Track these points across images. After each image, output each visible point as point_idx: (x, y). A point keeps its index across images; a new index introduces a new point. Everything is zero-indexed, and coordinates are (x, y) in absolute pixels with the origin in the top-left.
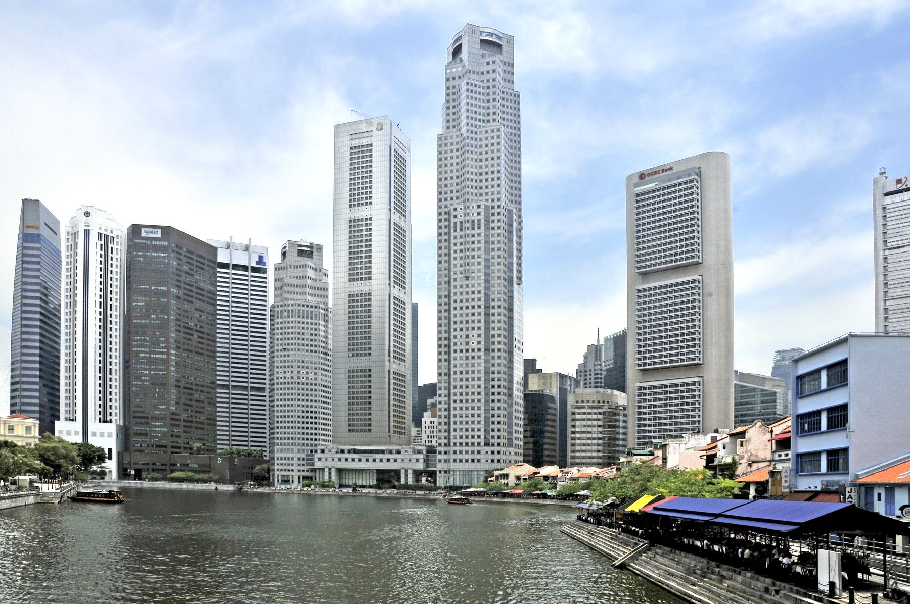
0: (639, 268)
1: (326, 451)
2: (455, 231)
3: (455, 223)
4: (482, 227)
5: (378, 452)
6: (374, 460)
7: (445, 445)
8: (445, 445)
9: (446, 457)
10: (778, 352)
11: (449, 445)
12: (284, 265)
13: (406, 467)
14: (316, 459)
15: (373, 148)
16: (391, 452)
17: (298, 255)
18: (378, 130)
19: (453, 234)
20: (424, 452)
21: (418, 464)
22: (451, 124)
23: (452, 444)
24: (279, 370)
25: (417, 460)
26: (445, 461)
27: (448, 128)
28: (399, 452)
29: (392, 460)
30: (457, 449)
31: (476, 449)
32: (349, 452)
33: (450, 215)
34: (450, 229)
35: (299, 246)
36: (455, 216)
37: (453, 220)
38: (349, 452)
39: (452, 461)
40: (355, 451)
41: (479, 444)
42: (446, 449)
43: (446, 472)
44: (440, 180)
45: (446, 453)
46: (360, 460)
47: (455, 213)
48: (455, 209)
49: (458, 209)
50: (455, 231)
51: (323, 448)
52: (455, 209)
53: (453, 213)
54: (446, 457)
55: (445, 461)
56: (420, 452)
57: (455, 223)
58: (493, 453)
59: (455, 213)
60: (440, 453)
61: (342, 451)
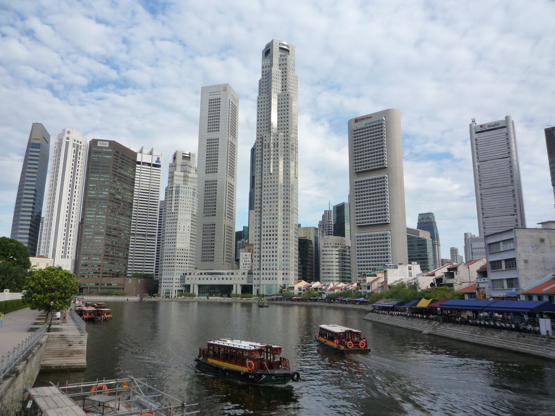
1: (192, 274)
2: (265, 148)
3: (265, 144)
4: (279, 147)
5: (220, 274)
6: (219, 279)
8: (258, 269)
9: (258, 276)
10: (420, 215)
14: (186, 279)
15: (221, 101)
16: (228, 274)
19: (264, 150)
20: (246, 274)
24: (169, 225)
25: (243, 279)
26: (258, 279)
28: (232, 274)
32: (205, 274)
34: (262, 147)
36: (265, 140)
37: (264, 142)
38: (205, 274)
40: (209, 274)
42: (258, 272)
43: (258, 285)
45: (258, 274)
46: (211, 279)
47: (265, 139)
48: (266, 137)
50: (265, 148)
51: (190, 272)
52: (266, 137)
53: (264, 139)
54: (258, 276)
55: (258, 279)
56: (244, 274)
57: (265, 144)
58: (283, 274)
59: (265, 139)
60: (255, 274)
61: (201, 274)
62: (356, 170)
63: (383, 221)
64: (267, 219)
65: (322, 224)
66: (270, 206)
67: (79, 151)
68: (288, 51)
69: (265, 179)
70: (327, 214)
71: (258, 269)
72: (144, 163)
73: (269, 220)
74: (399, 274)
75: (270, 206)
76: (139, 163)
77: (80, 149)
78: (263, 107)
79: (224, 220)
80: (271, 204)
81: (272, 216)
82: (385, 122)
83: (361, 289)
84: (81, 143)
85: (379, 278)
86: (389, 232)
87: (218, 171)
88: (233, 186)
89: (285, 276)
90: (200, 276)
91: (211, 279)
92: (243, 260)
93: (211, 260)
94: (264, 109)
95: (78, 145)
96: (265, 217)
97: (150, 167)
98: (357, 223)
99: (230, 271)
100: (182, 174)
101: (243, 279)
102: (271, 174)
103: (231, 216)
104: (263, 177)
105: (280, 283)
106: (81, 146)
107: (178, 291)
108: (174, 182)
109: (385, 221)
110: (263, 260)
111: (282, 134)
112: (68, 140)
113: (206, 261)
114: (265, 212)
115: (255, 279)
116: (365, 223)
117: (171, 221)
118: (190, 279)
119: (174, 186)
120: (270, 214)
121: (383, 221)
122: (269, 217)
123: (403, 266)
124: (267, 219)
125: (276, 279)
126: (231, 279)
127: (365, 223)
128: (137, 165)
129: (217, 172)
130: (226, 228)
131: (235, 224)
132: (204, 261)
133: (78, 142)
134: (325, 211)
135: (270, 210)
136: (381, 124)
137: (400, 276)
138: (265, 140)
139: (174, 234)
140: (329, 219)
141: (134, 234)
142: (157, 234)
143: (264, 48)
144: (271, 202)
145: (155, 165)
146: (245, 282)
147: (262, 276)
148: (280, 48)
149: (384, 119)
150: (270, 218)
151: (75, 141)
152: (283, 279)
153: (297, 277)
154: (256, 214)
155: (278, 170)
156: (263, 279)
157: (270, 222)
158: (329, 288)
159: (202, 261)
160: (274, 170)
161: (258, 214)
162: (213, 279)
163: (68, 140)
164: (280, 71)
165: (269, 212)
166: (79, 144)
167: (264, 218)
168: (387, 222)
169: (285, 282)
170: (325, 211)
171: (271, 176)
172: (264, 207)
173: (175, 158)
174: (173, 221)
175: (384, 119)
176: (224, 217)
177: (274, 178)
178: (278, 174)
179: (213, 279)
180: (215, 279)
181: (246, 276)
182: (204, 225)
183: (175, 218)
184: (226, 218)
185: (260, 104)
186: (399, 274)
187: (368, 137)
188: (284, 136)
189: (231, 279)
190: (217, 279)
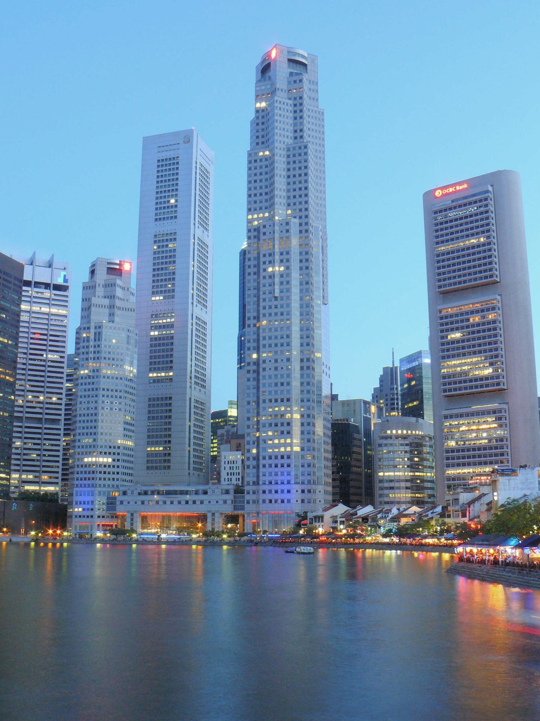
0: (440, 287)
1: (129, 492)
5: (182, 493)
7: (254, 483)
9: (254, 497)
11: (258, 484)
12: (93, 284)
13: (213, 510)
16: (197, 493)
17: (108, 273)
18: (185, 142)
20: (232, 492)
21: (226, 506)
22: (260, 140)
23: (261, 483)
24: (83, 400)
26: (254, 502)
27: (258, 144)
28: (205, 493)
29: (198, 503)
30: (267, 488)
31: (286, 487)
33: (259, 232)
35: (109, 263)
39: (261, 501)
41: (289, 482)
42: (254, 488)
44: (250, 196)
45: (254, 493)
49: (267, 226)
54: (254, 497)
55: (254, 502)
56: (227, 492)
58: (303, 491)
60: (248, 493)
62: (440, 287)
63: (493, 385)
64: (270, 385)
65: (377, 395)
68: (305, 65)
69: (264, 308)
70: (389, 375)
71: (254, 483)
72: (37, 284)
73: (273, 389)
74: (520, 486)
76: (28, 283)
78: (258, 171)
79: (188, 390)
81: (279, 380)
82: (491, 196)
83: (449, 516)
85: (484, 495)
86: (505, 406)
87: (176, 294)
88: (205, 323)
89: (306, 496)
90: (143, 498)
91: (165, 503)
92: (227, 466)
93: (165, 468)
94: (261, 174)
96: (267, 381)
97: (48, 291)
98: (445, 391)
99: (201, 488)
100: (106, 302)
101: (225, 502)
102: (276, 298)
103: (202, 382)
104: (262, 304)
105: (298, 508)
107: (103, 525)
108: (93, 317)
109: (498, 384)
110: (264, 466)
111: (297, 221)
113: (156, 468)
114: (266, 373)
115: (248, 502)
116: (460, 389)
117: (87, 393)
118: (125, 503)
119: (93, 325)
120: (276, 376)
121: (493, 385)
122: (273, 381)
123: (528, 470)
124: (270, 385)
125: (289, 501)
126: (202, 502)
127: (460, 389)
128: (24, 288)
129: (173, 297)
130: (193, 404)
131: (210, 397)
132: (152, 468)
134: (385, 369)
135: (276, 369)
136: (486, 199)
137: (522, 489)
138: (264, 234)
139: (94, 418)
140: (392, 383)
141: (20, 419)
142: (62, 418)
143: (259, 61)
145: (57, 287)
146: (229, 509)
147: (262, 497)
148: (290, 60)
149: (490, 189)
150: (276, 384)
152: (303, 501)
153: (330, 498)
154: (248, 376)
155: (288, 290)
156: (264, 501)
157: (276, 392)
158: (390, 516)
159: (148, 468)
160: (282, 292)
161: (252, 375)
162: (168, 502)
164: (291, 102)
165: (272, 372)
167: (264, 385)
168: (501, 387)
169: (307, 507)
170: (385, 369)
171: (276, 303)
173: (93, 272)
174: (91, 393)
175: (490, 189)
176: (188, 384)
177: (282, 307)
178: (288, 298)
179: (168, 502)
180: (172, 503)
181: (230, 497)
182: (150, 400)
183: (95, 386)
184: (193, 386)
185: (253, 165)
186: (520, 486)
187: (461, 225)
188: (300, 224)
189: (202, 502)
190: (176, 502)
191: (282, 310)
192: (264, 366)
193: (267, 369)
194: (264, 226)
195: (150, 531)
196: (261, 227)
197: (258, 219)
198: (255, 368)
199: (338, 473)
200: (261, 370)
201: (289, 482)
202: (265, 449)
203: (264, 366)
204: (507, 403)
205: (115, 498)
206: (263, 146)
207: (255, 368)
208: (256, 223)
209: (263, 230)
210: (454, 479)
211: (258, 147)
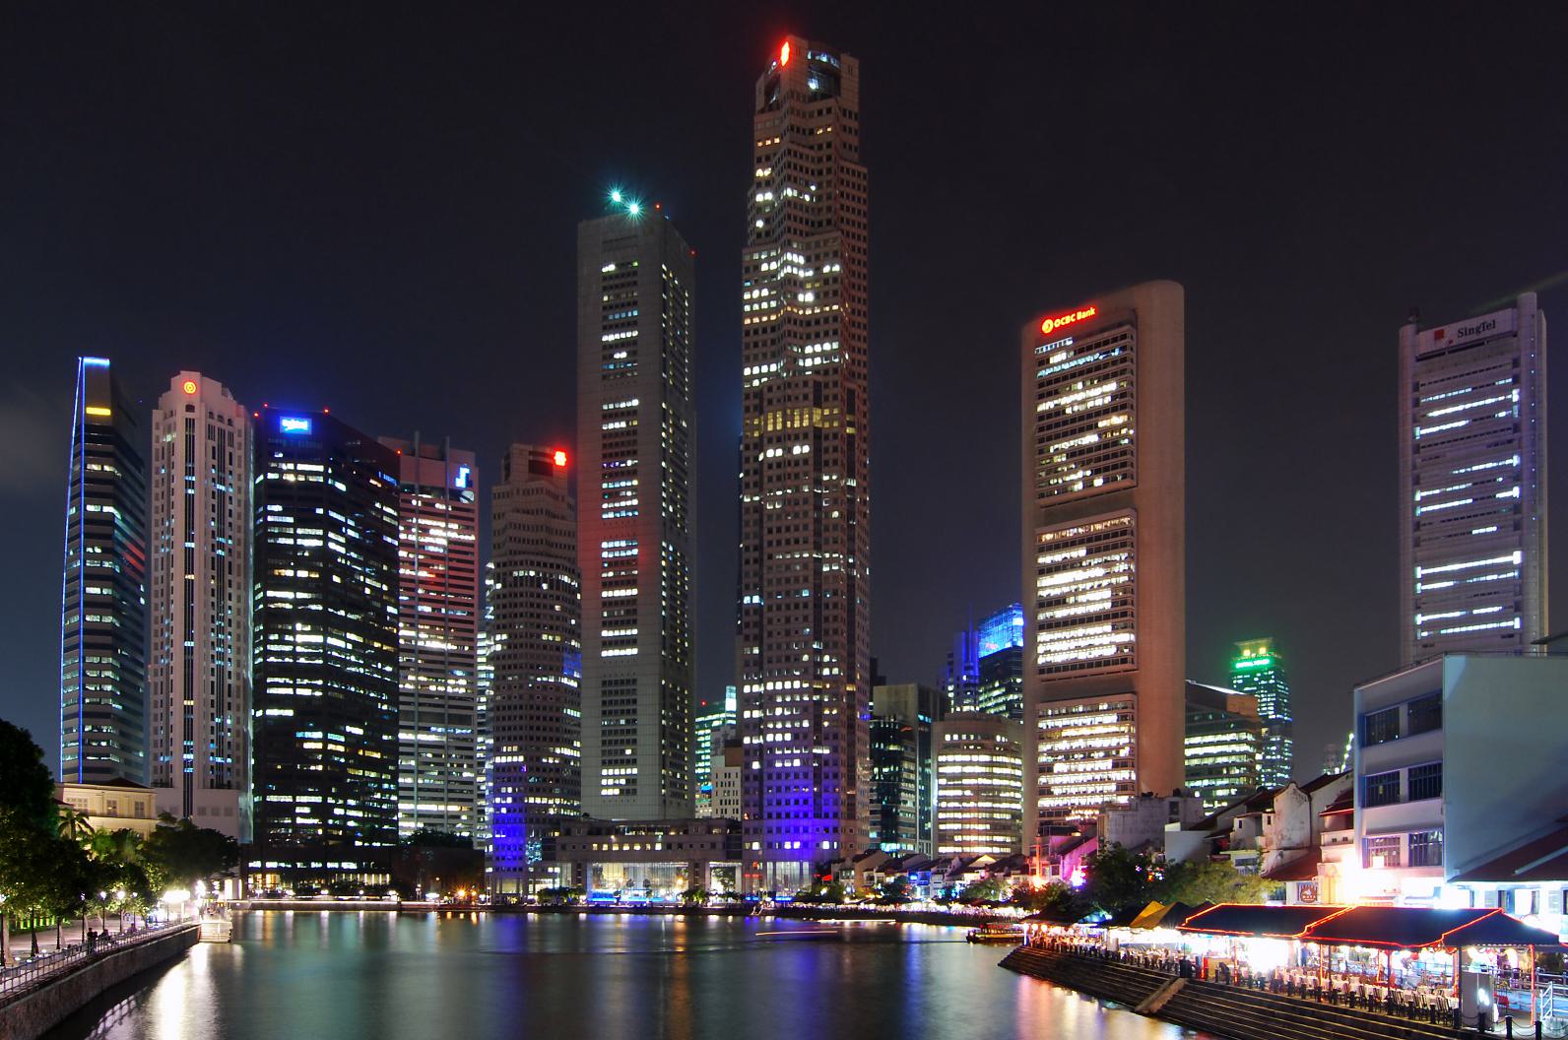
66: (788, 620)
67: (228, 449)
69: (770, 531)
75: (788, 620)
77: (232, 446)
80: (788, 613)
84: (230, 422)
95: (222, 432)
106: (231, 435)
112: (190, 415)
114: (774, 640)
133: (221, 418)
144: (788, 607)
151: (211, 414)
163: (190, 415)
166: (224, 426)
172: (770, 621)
173: (508, 468)
191: (796, 534)
192: (770, 628)
193: (775, 633)
194: (770, 389)
195: (605, 891)
196: (765, 390)
197: (760, 376)
198: (757, 618)
199: (879, 801)
200: (765, 635)
201: (806, 815)
202: (771, 764)
203: (770, 628)
204: (1134, 693)
205: (554, 838)
206: (768, 239)
207: (757, 618)
208: (756, 383)
209: (767, 396)
210: (1050, 814)
211: (760, 240)
